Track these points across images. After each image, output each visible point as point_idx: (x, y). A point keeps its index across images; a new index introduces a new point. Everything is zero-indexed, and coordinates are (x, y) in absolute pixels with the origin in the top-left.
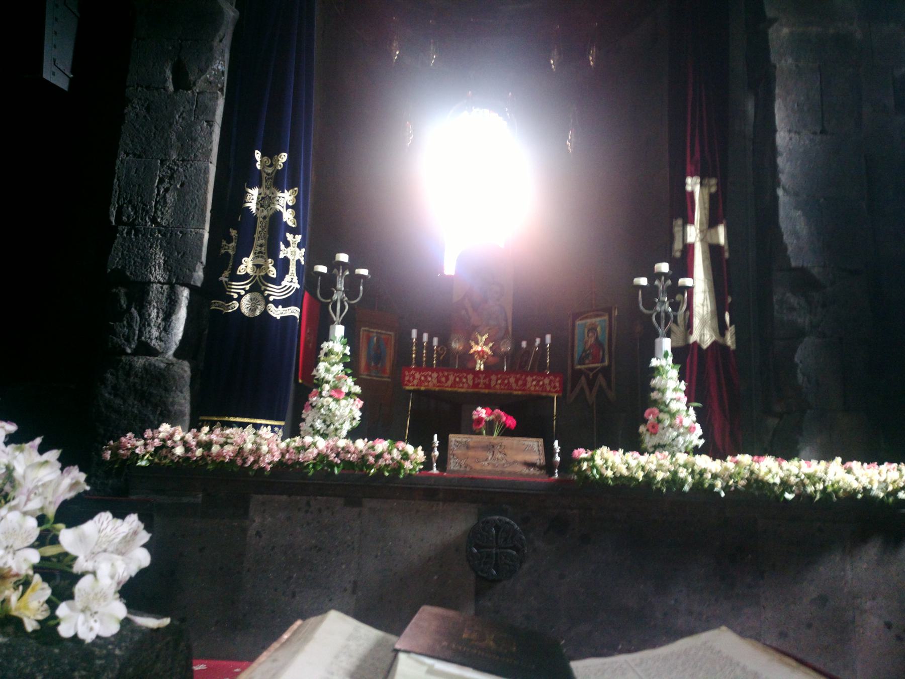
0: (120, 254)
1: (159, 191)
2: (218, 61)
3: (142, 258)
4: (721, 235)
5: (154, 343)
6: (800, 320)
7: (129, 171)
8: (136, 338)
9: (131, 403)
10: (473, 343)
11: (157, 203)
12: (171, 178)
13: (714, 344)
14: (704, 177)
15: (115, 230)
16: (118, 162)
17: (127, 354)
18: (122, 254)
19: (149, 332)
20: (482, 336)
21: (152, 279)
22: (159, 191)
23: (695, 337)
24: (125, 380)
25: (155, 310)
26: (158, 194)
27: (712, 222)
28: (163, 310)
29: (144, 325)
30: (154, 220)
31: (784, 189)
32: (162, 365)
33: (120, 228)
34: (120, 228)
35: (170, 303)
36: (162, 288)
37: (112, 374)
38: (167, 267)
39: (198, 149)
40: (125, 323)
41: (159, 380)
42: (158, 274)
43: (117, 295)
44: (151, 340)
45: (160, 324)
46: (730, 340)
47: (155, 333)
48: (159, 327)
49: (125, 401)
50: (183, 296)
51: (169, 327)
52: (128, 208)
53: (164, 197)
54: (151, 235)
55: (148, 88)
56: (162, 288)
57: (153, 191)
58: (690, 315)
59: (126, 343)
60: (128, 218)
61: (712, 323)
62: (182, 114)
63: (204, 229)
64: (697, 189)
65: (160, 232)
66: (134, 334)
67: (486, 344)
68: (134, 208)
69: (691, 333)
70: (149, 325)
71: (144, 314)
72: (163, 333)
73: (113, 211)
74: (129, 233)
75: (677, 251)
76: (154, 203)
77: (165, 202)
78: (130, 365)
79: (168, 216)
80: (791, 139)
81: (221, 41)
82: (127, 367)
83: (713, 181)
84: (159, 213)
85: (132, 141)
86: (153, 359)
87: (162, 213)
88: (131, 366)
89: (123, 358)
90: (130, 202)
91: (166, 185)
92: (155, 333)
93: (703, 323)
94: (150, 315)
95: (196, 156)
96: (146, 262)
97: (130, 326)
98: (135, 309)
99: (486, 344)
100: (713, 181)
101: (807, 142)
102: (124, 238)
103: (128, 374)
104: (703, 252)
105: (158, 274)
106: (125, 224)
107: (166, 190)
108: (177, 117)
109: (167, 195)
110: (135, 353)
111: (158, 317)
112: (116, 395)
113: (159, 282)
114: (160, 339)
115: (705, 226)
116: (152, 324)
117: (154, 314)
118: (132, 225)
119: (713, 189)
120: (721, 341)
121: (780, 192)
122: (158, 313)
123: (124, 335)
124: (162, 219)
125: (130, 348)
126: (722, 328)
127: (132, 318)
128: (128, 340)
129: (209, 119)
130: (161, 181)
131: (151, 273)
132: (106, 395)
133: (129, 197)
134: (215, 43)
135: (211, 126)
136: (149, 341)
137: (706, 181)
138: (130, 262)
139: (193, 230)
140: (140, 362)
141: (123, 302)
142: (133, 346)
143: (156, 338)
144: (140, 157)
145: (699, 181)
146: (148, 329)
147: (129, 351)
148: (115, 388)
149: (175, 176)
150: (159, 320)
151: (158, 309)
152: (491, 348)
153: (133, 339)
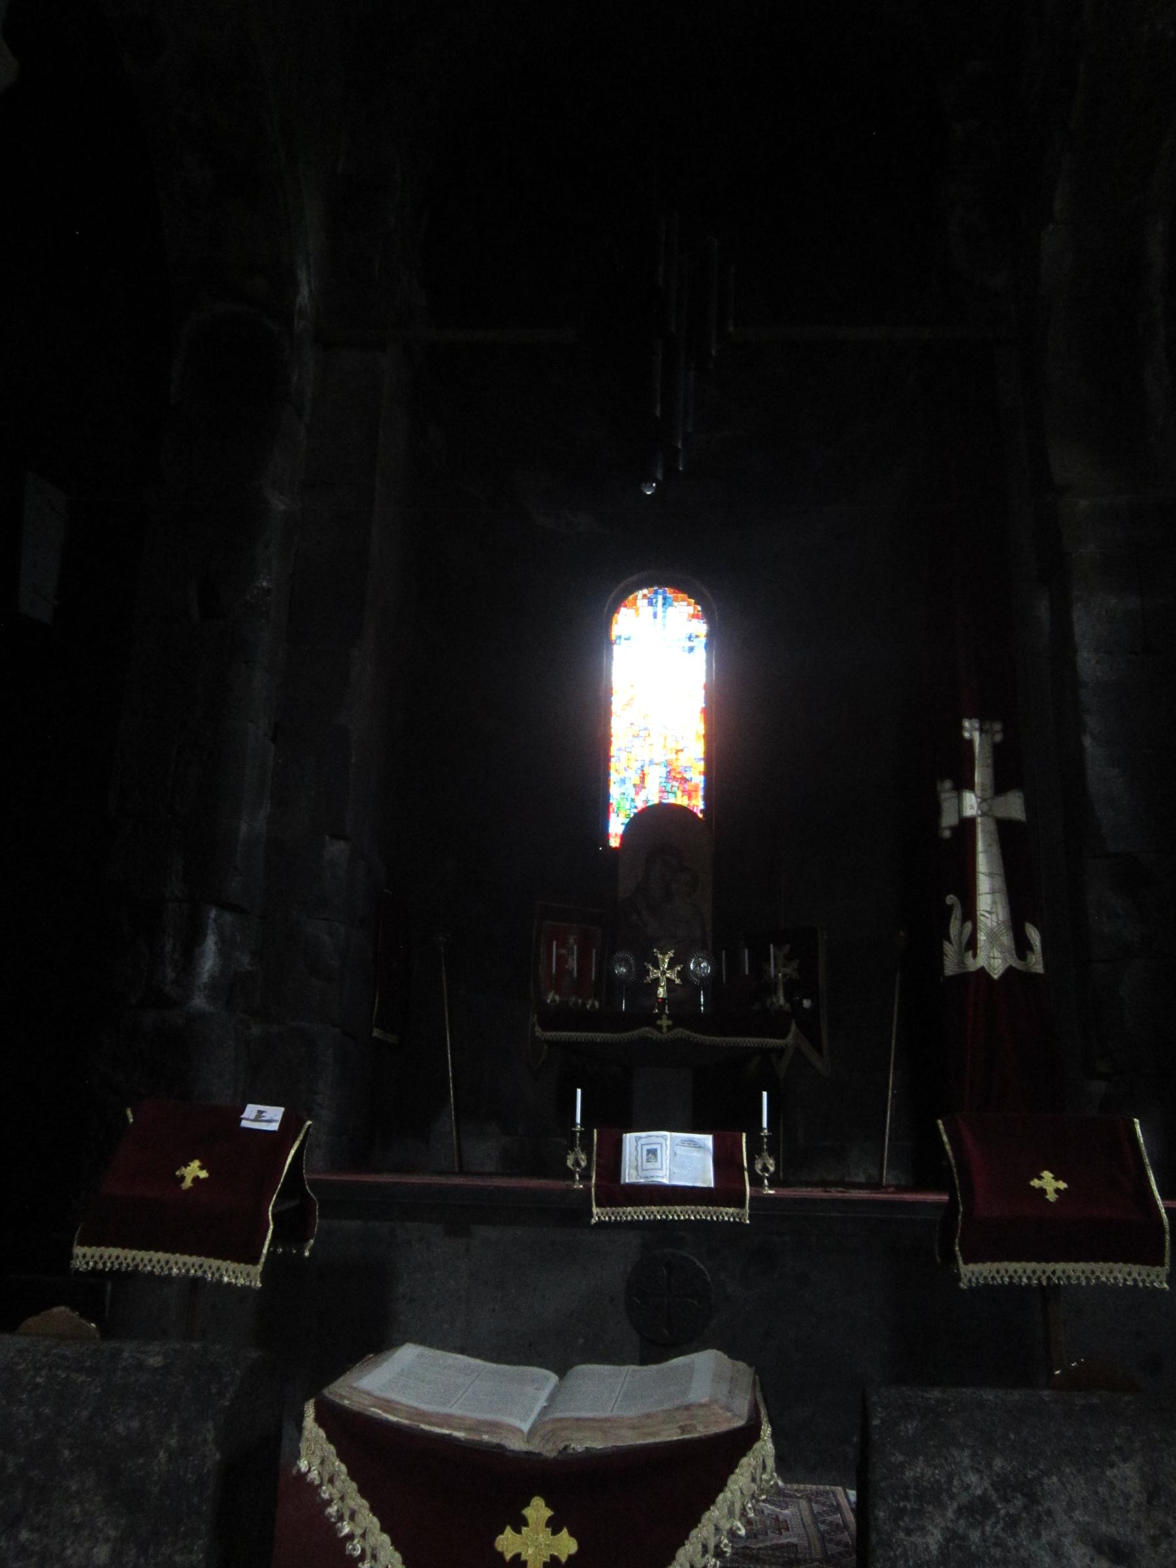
2: (261, 576)
4: (1014, 806)
13: (1010, 972)
14: (984, 717)
20: (664, 954)
23: (981, 961)
27: (1001, 784)
46: (1036, 963)
47: (171, 974)
50: (209, 918)
61: (1007, 939)
64: (976, 736)
67: (671, 967)
69: (975, 955)
83: (997, 726)
92: (171, 974)
93: (993, 937)
100: (997, 726)
115: (989, 793)
117: (169, 947)
119: (998, 738)
126: (1022, 946)
137: (987, 727)
145: (977, 725)
150: (176, 956)
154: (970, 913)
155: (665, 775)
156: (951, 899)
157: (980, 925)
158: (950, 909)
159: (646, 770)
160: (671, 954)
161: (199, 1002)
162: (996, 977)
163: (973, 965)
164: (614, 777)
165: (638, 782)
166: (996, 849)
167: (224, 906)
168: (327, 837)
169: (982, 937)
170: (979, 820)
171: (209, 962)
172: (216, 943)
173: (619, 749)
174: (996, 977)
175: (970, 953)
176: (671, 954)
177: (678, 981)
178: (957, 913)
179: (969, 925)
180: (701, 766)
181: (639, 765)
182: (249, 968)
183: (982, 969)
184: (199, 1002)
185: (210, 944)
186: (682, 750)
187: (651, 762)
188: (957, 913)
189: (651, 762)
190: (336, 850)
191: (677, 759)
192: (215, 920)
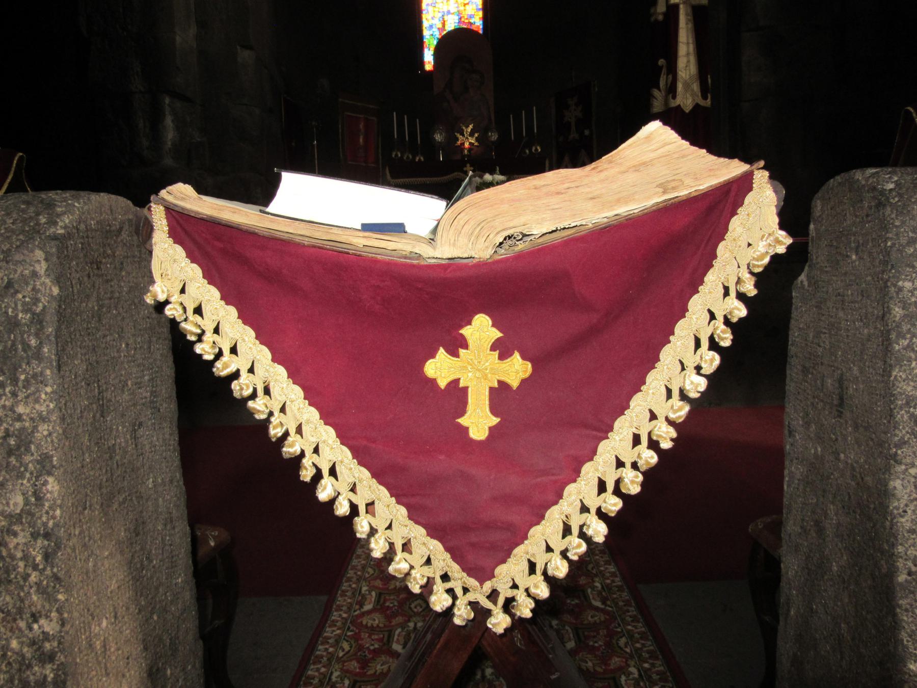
10: (458, 135)
13: (697, 106)
20: (467, 127)
58: (671, 83)
61: (696, 87)
67: (472, 134)
69: (674, 97)
75: (659, 14)
93: (687, 86)
99: (472, 134)
104: (687, 14)
117: (141, 125)
120: (702, 103)
152: (477, 140)
154: (672, 69)
155: (457, 21)
156: (661, 62)
157: (679, 77)
158: (661, 68)
159: (446, 18)
160: (471, 127)
162: (687, 111)
163: (673, 104)
164: (425, 24)
165: (440, 26)
166: (690, 25)
168: (238, 47)
169: (680, 86)
170: (681, 6)
171: (170, 135)
172: (173, 121)
173: (428, 5)
174: (687, 111)
175: (671, 95)
176: (471, 127)
177: (476, 144)
178: (664, 70)
179: (670, 77)
180: (480, 14)
181: (440, 15)
182: (199, 140)
183: (679, 106)
185: (169, 121)
186: (468, 4)
187: (449, 12)
188: (664, 70)
189: (449, 12)
190: (245, 56)
191: (465, 10)
192: (169, 105)
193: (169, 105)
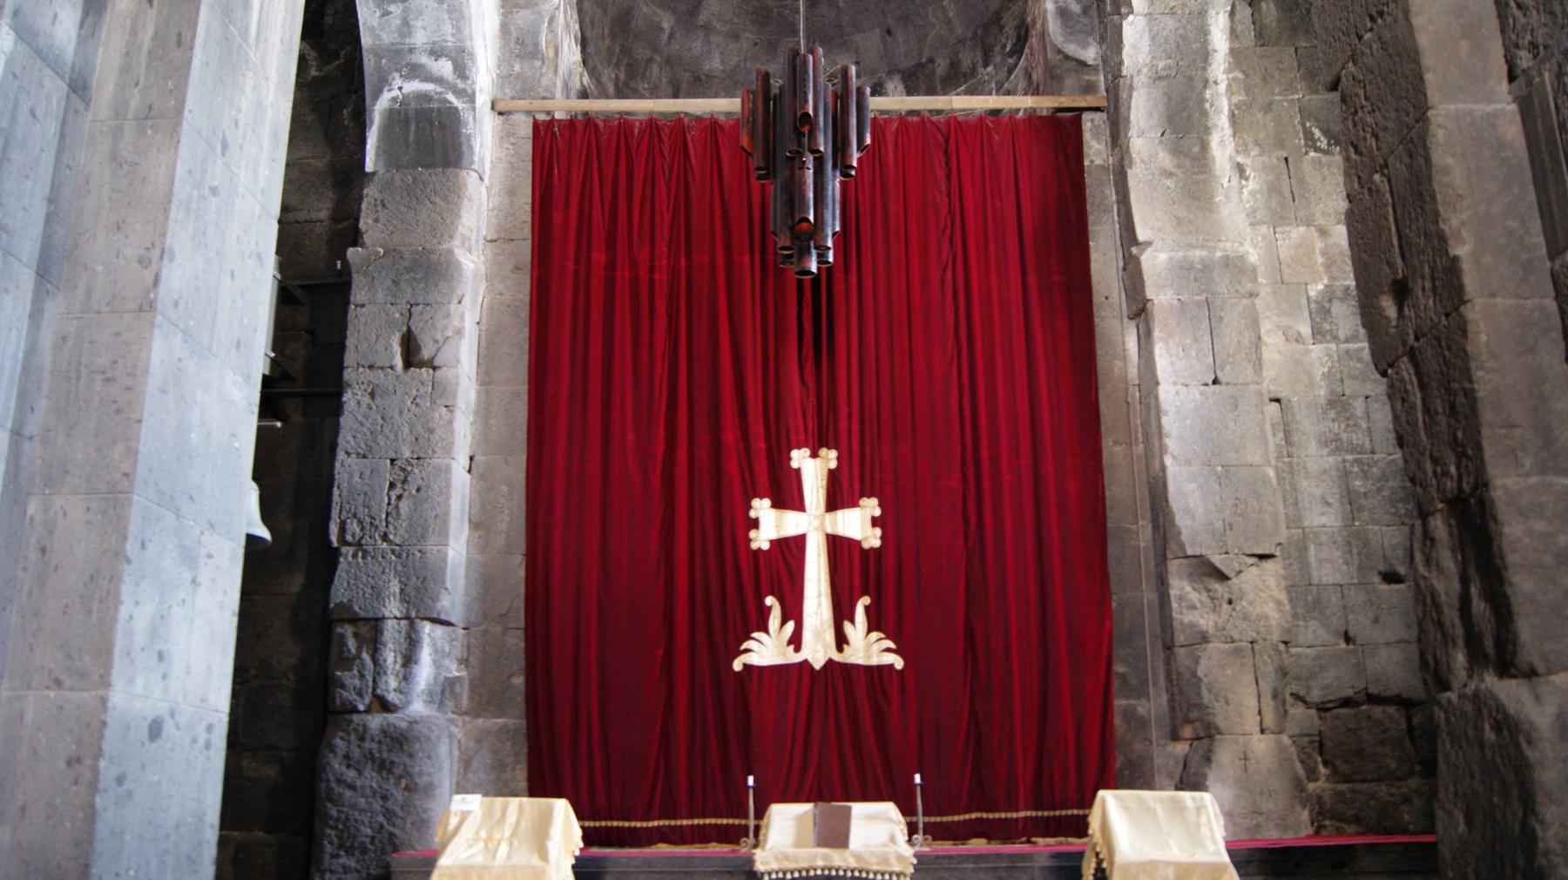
0: (345, 584)
1: (389, 499)
3: (372, 588)
5: (392, 697)
6: (1202, 622)
7: (351, 477)
8: (370, 690)
9: (368, 776)
11: (387, 514)
12: (405, 481)
15: (337, 552)
16: (338, 465)
17: (359, 712)
18: (348, 583)
19: (386, 682)
21: (387, 614)
22: (389, 499)
24: (359, 746)
25: (392, 654)
26: (389, 504)
28: (401, 653)
29: (379, 673)
30: (385, 538)
31: (1174, 457)
32: (404, 725)
33: (344, 550)
34: (344, 550)
35: (410, 644)
36: (399, 624)
37: (342, 738)
38: (404, 597)
39: (437, 442)
40: (356, 672)
41: (401, 745)
42: (393, 608)
43: (342, 636)
44: (389, 692)
45: (399, 672)
47: (393, 683)
48: (397, 676)
49: (360, 772)
51: (410, 674)
52: (352, 523)
53: (397, 507)
54: (383, 557)
55: (371, 367)
56: (399, 624)
57: (383, 500)
59: (358, 698)
60: (353, 535)
62: (414, 399)
63: (446, 545)
65: (393, 552)
66: (367, 687)
68: (360, 522)
70: (385, 673)
71: (378, 659)
72: (403, 684)
73: (334, 529)
74: (355, 556)
76: (384, 516)
77: (398, 514)
78: (365, 726)
79: (402, 532)
80: (1177, 393)
81: (460, 302)
82: (361, 729)
84: (391, 527)
85: (354, 437)
86: (391, 717)
87: (395, 528)
88: (365, 728)
89: (355, 717)
90: (355, 515)
91: (398, 491)
92: (393, 683)
94: (385, 661)
95: (434, 452)
96: (378, 594)
97: (362, 676)
98: (367, 653)
101: (1198, 396)
102: (350, 563)
103: (362, 738)
105: (393, 608)
106: (350, 545)
107: (399, 497)
108: (409, 403)
109: (401, 504)
110: (368, 711)
111: (395, 662)
112: (348, 766)
113: (396, 618)
114: (398, 690)
116: (389, 672)
118: (359, 544)
121: (1168, 460)
122: (395, 657)
123: (355, 688)
124: (395, 534)
125: (363, 704)
127: (363, 664)
128: (360, 694)
129: (449, 403)
130: (392, 485)
131: (384, 606)
132: (337, 766)
133: (353, 508)
134: (453, 307)
135: (452, 412)
136: (386, 694)
138: (357, 593)
139: (434, 548)
140: (375, 721)
141: (352, 644)
142: (367, 701)
143: (395, 690)
144: (365, 457)
146: (384, 678)
147: (361, 708)
148: (347, 757)
149: (409, 479)
150: (398, 667)
151: (395, 651)
153: (367, 693)
161: (418, 707)
167: (437, 621)
171: (425, 672)
184: (418, 707)
193: (429, 635)
